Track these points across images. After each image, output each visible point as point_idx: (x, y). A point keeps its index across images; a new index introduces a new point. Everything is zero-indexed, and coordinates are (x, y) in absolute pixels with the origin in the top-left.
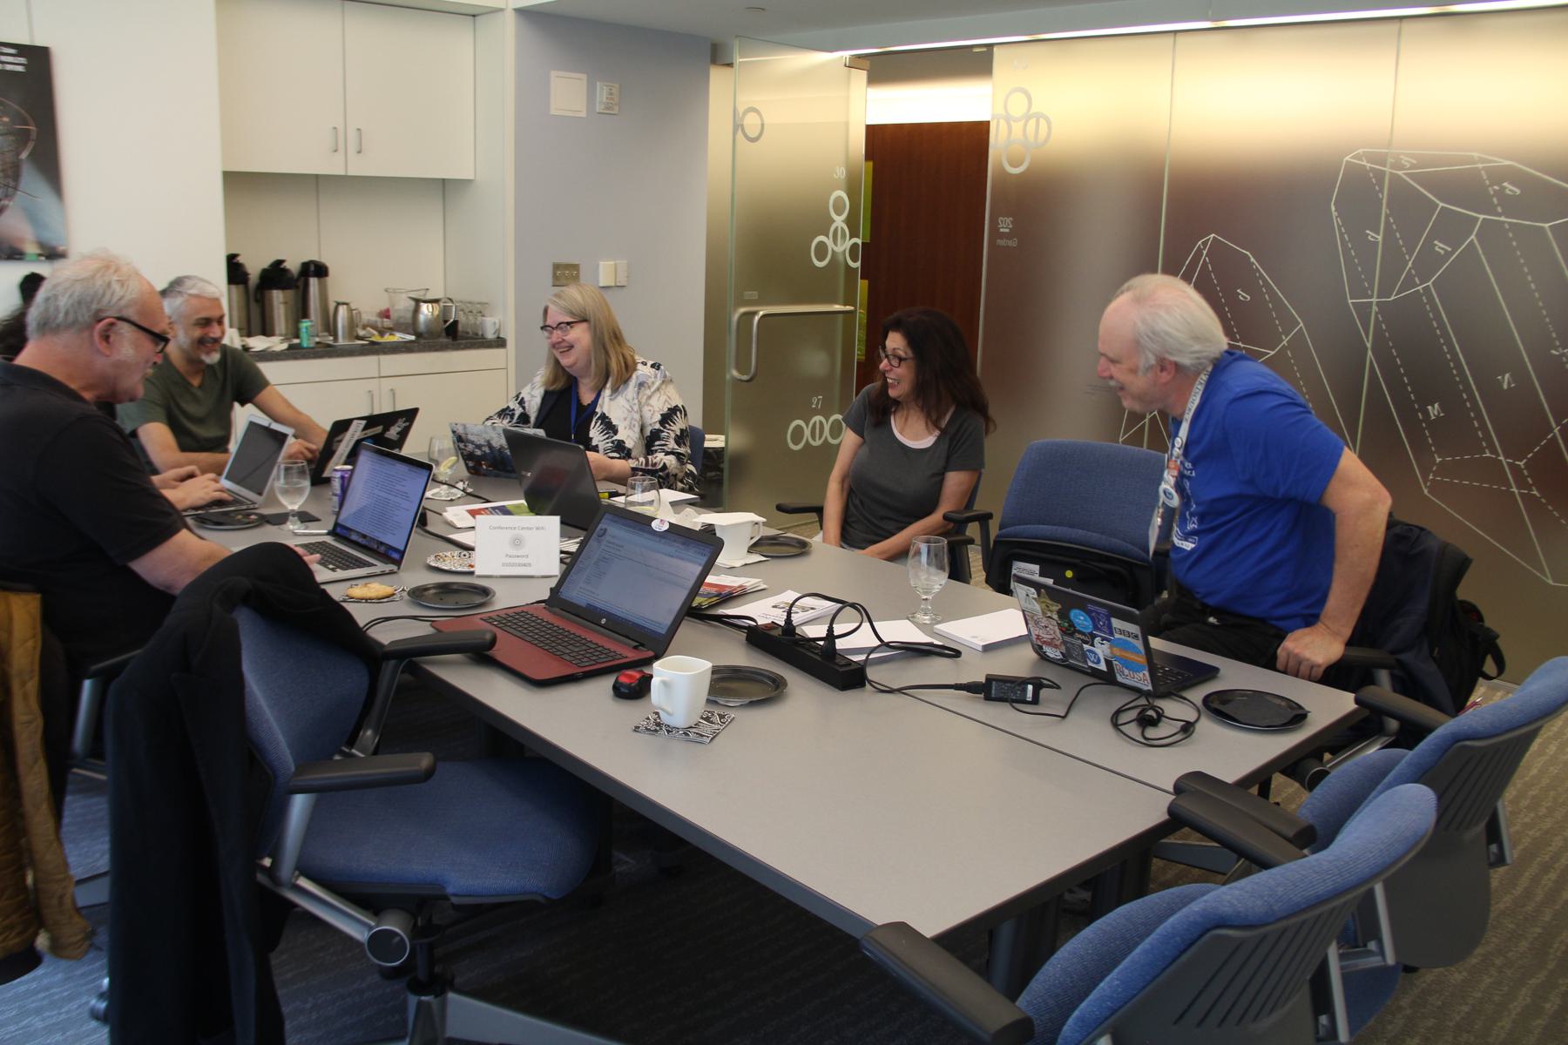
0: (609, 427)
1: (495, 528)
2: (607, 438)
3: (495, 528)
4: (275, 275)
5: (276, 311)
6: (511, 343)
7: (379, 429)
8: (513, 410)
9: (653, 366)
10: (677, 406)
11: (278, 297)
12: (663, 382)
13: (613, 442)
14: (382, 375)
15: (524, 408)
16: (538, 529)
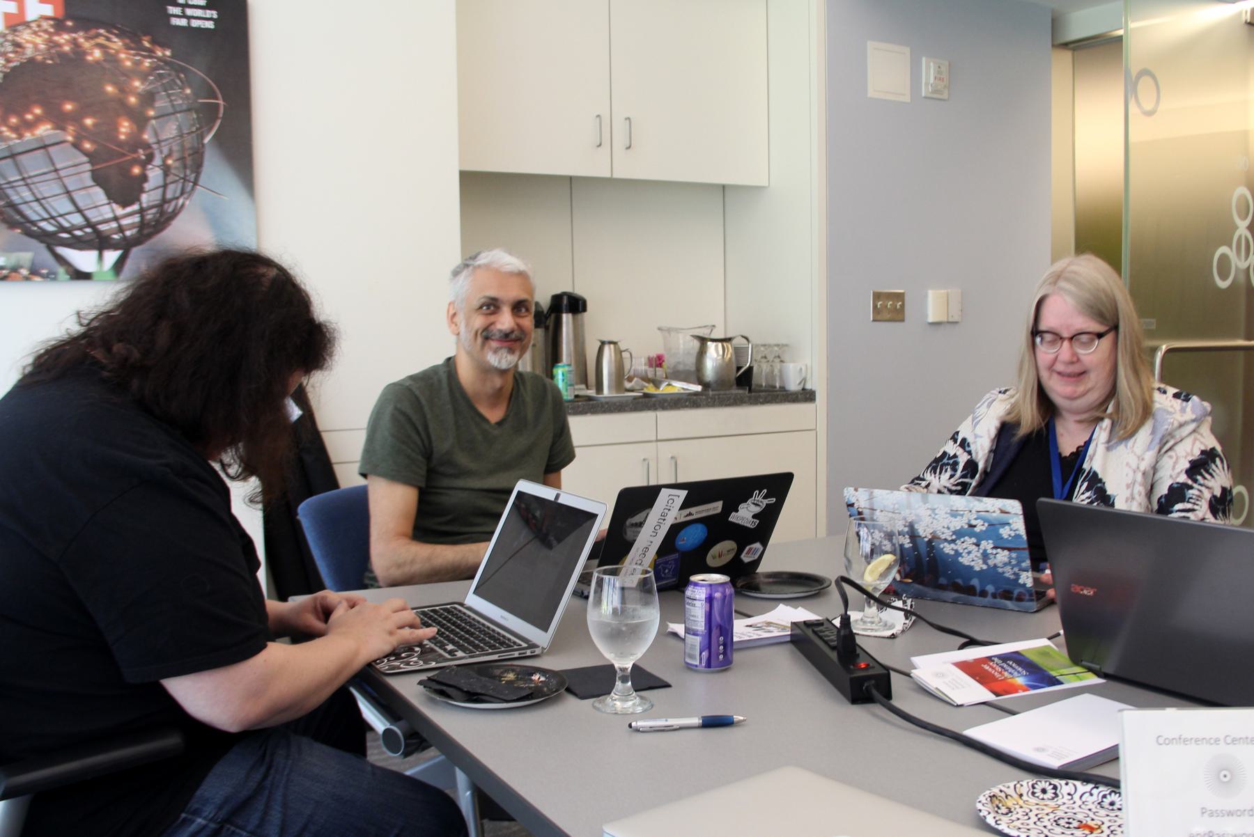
6: (821, 397)
7: (716, 507)
15: (970, 453)
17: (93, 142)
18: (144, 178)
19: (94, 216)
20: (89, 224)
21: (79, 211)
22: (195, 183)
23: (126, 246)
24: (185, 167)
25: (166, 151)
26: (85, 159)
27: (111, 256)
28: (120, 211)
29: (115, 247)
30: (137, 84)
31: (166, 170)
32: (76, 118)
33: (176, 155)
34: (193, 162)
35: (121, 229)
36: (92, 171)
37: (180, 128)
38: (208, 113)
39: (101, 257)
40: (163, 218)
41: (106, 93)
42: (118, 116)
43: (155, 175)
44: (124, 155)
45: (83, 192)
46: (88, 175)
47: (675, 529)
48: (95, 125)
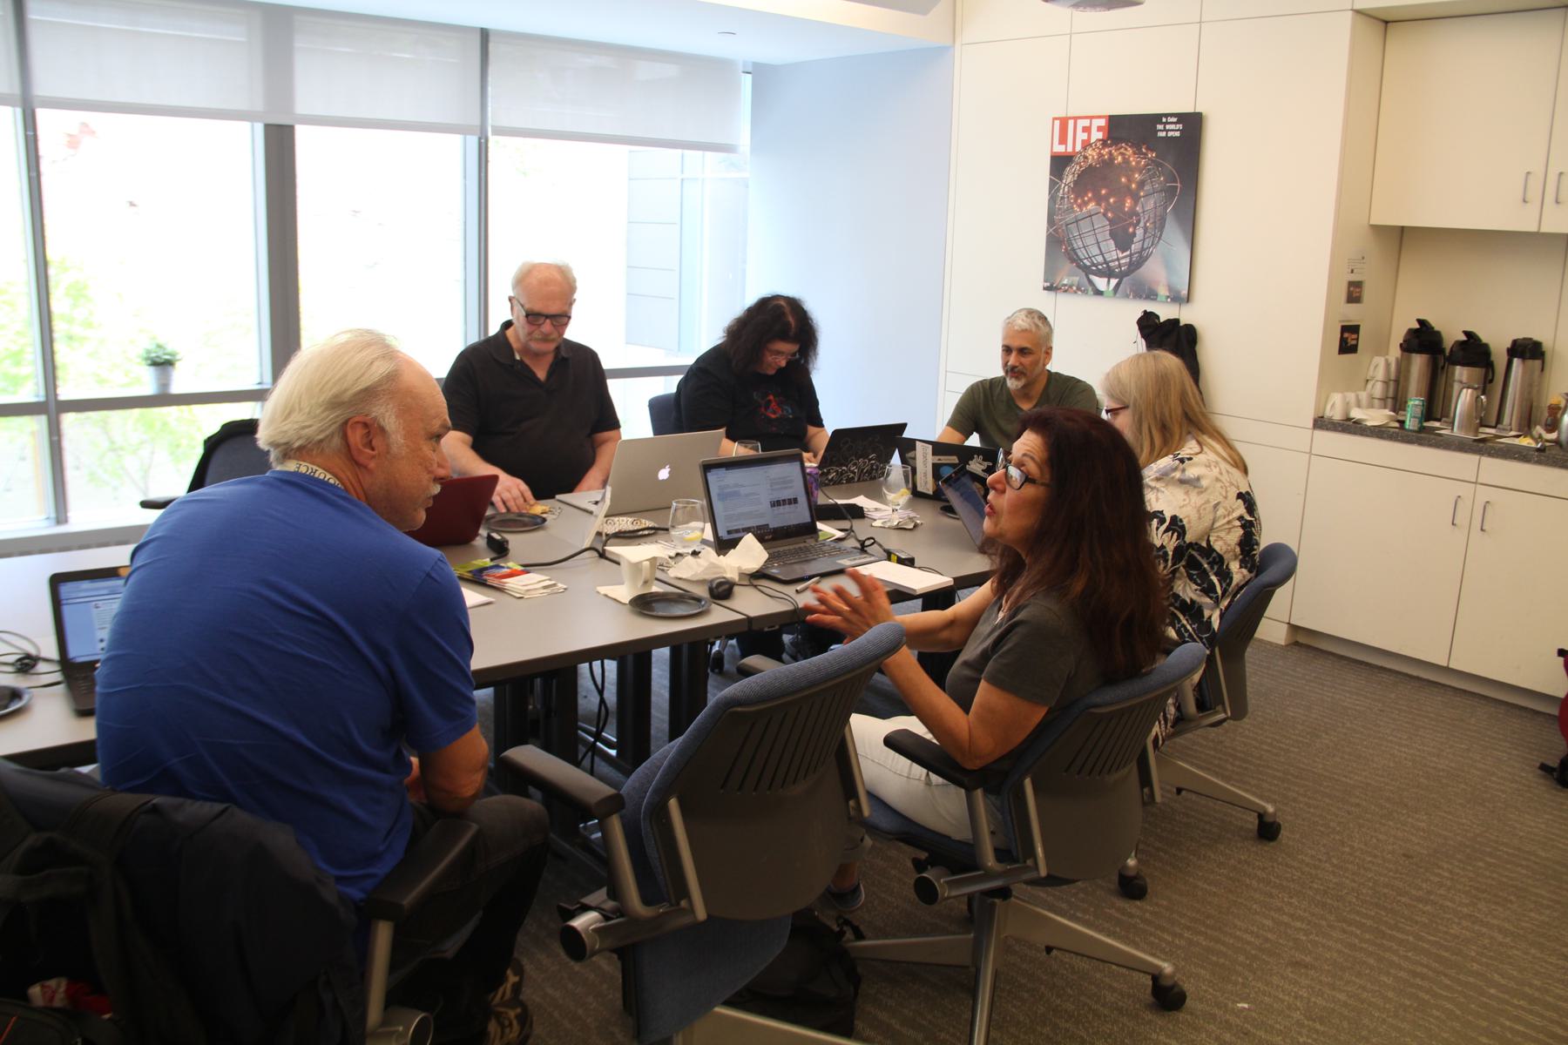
4: (1473, 351)
10: (1162, 512)
11: (1461, 373)
17: (1113, 212)
18: (1134, 234)
20: (1106, 262)
21: (1102, 254)
22: (1160, 238)
23: (1121, 276)
27: (1114, 282)
28: (1121, 255)
29: (1116, 277)
30: (1137, 176)
31: (1146, 229)
32: (1106, 198)
33: (1151, 221)
34: (1160, 224)
35: (1120, 266)
36: (1110, 230)
37: (1155, 203)
39: (1109, 281)
41: (1120, 180)
43: (1140, 232)
45: (1104, 243)
46: (1108, 232)
48: (1114, 202)
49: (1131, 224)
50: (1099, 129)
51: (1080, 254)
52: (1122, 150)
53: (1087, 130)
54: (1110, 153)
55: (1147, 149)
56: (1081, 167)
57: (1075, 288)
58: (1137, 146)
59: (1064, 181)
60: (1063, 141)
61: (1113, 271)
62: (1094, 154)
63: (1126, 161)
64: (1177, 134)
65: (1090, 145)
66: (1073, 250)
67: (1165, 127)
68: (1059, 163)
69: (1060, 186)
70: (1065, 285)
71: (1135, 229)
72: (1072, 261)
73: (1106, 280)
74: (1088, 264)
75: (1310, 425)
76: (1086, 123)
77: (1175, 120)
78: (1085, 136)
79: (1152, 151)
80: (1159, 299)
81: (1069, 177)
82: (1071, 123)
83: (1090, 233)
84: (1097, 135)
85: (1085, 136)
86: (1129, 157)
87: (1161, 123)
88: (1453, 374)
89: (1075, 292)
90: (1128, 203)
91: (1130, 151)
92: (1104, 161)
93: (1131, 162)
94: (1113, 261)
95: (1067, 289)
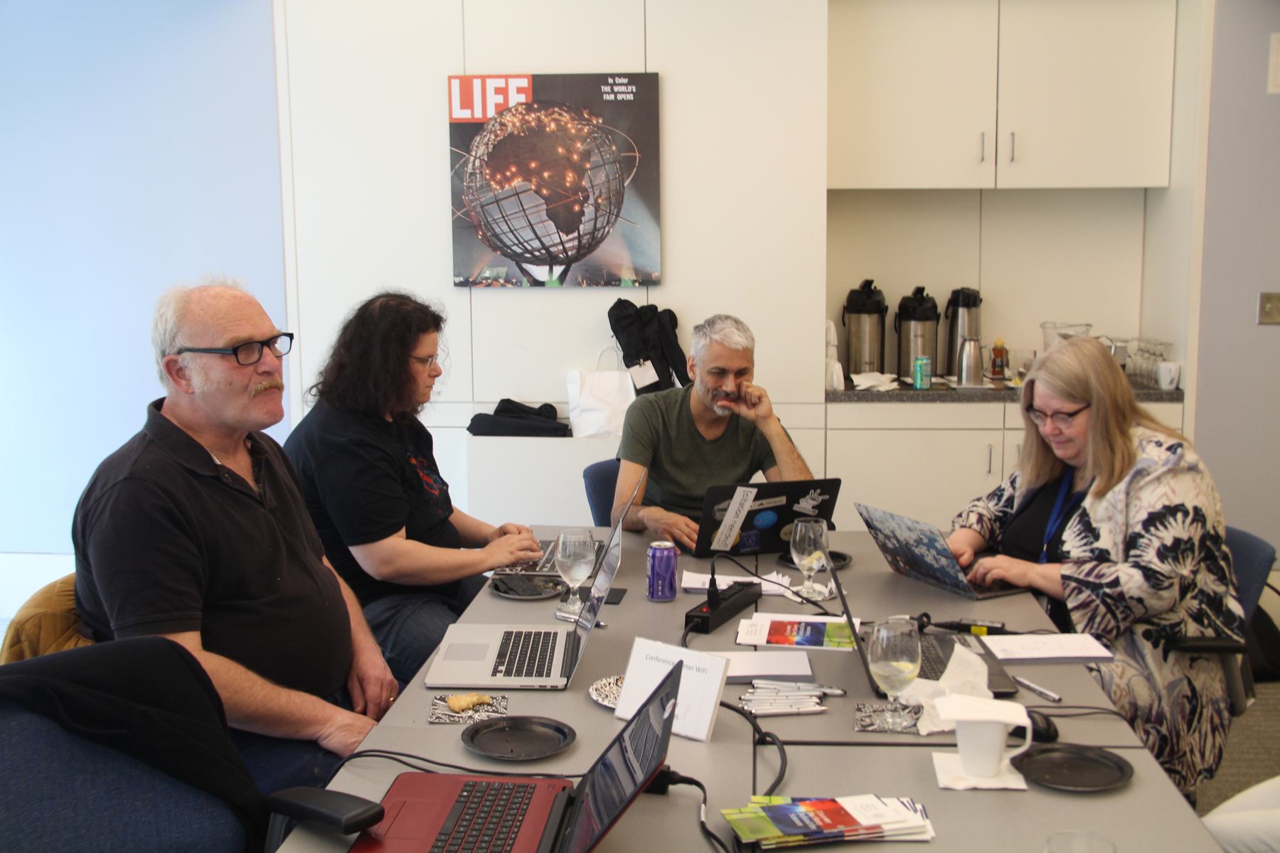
0: (1090, 532)
1: (652, 658)
2: (1085, 545)
3: (652, 658)
4: (917, 305)
5: (912, 345)
7: (782, 500)
8: (1004, 490)
9: (1169, 449)
11: (915, 328)
12: (1170, 471)
13: (1092, 551)
14: (824, 426)
16: (698, 670)
17: (548, 189)
18: (582, 213)
19: (547, 241)
21: (538, 238)
22: (617, 216)
23: (568, 262)
24: (610, 204)
25: (597, 193)
26: (543, 201)
27: (558, 270)
28: (564, 238)
29: (561, 264)
30: (579, 145)
31: (597, 207)
32: (538, 173)
33: (604, 196)
34: (617, 200)
35: (565, 250)
36: (547, 210)
37: (607, 176)
38: (627, 164)
39: (551, 270)
40: (594, 241)
42: (565, 169)
43: (589, 210)
44: (569, 197)
46: (545, 212)
47: (751, 515)
48: (549, 177)
49: (576, 202)
50: (520, 90)
51: (506, 240)
52: (556, 116)
53: (502, 91)
54: (539, 119)
55: (590, 114)
56: (497, 136)
57: (502, 281)
58: (576, 112)
59: (474, 153)
60: (467, 102)
61: (557, 256)
62: (516, 120)
63: (562, 128)
64: (630, 97)
65: (509, 110)
66: (496, 236)
67: (612, 89)
68: (463, 134)
69: (468, 159)
70: (487, 278)
71: (582, 206)
72: (495, 248)
73: (547, 268)
74: (519, 251)
75: (823, 400)
76: (501, 83)
77: (625, 81)
78: (500, 99)
79: (597, 116)
80: (623, 284)
81: (481, 147)
82: (477, 84)
83: (520, 214)
84: (516, 99)
85: (500, 99)
86: (566, 123)
87: (607, 84)
88: (909, 328)
89: (503, 285)
90: (570, 177)
91: (566, 117)
92: (531, 129)
93: (569, 129)
94: (555, 245)
95: (491, 283)
